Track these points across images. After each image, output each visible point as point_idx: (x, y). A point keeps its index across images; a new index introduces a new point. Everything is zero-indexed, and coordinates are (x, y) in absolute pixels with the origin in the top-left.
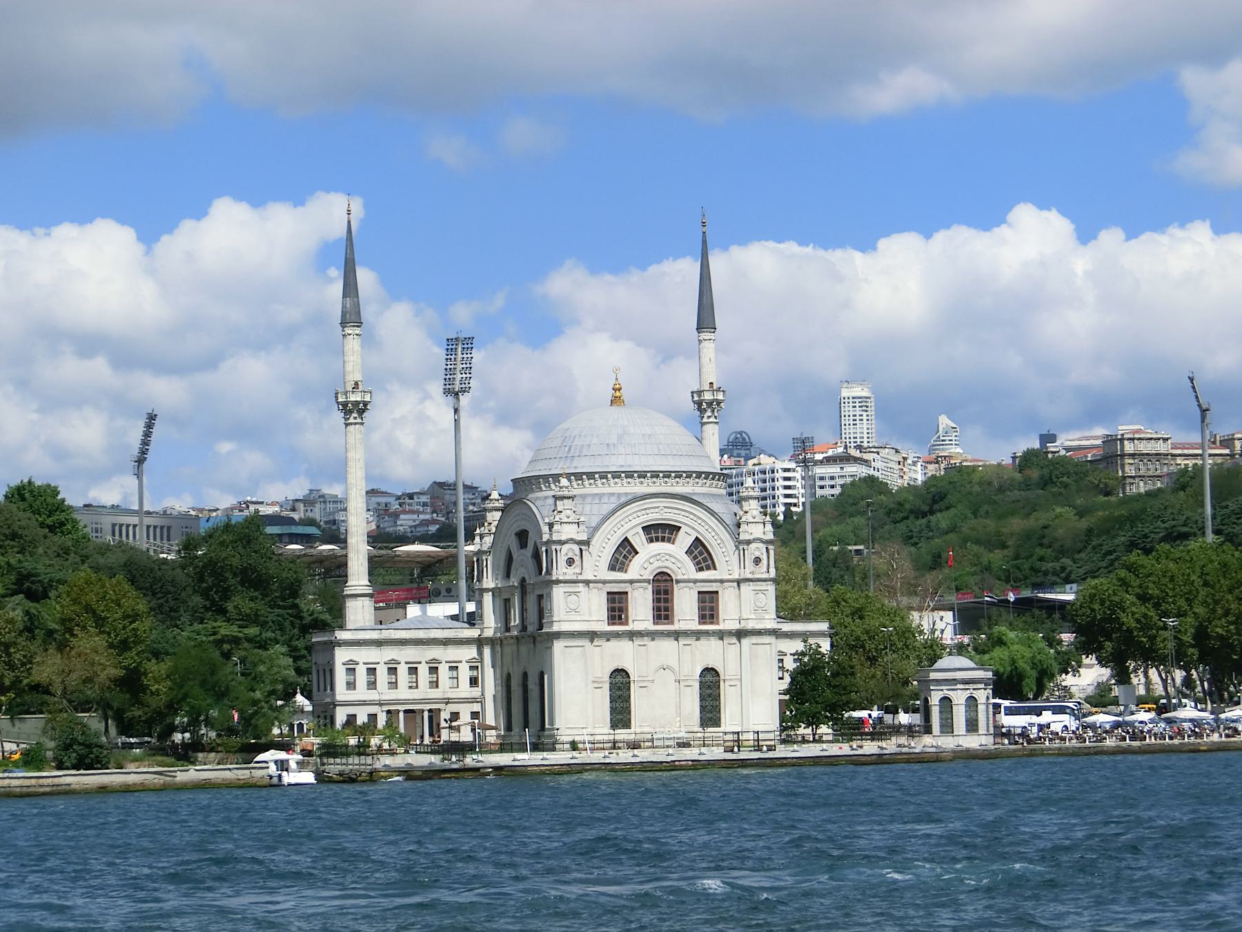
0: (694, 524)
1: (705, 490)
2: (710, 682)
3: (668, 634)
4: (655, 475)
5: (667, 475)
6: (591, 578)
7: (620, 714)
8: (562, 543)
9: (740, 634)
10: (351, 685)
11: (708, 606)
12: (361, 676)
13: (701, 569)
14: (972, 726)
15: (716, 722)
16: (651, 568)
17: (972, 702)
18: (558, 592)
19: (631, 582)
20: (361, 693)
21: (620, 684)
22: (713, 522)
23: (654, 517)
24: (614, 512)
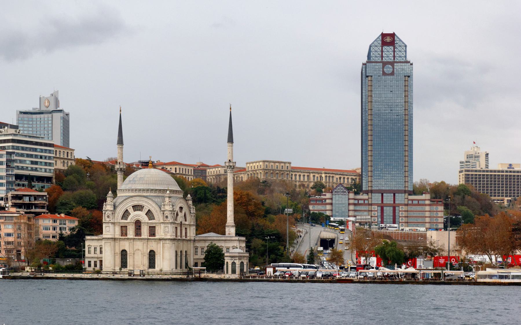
0: (149, 205)
1: (155, 194)
2: (152, 255)
3: (139, 239)
4: (136, 190)
5: (140, 190)
6: (115, 221)
7: (124, 264)
8: (106, 211)
9: (160, 239)
10: (89, 252)
11: (152, 231)
12: (92, 250)
13: (151, 220)
14: (234, 272)
15: (154, 267)
16: (134, 219)
17: (234, 264)
18: (104, 225)
19: (128, 223)
20: (92, 255)
21: (124, 254)
22: (154, 205)
23: (136, 203)
24: (123, 201)
